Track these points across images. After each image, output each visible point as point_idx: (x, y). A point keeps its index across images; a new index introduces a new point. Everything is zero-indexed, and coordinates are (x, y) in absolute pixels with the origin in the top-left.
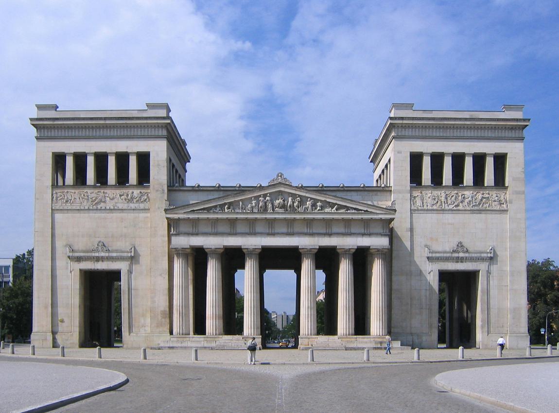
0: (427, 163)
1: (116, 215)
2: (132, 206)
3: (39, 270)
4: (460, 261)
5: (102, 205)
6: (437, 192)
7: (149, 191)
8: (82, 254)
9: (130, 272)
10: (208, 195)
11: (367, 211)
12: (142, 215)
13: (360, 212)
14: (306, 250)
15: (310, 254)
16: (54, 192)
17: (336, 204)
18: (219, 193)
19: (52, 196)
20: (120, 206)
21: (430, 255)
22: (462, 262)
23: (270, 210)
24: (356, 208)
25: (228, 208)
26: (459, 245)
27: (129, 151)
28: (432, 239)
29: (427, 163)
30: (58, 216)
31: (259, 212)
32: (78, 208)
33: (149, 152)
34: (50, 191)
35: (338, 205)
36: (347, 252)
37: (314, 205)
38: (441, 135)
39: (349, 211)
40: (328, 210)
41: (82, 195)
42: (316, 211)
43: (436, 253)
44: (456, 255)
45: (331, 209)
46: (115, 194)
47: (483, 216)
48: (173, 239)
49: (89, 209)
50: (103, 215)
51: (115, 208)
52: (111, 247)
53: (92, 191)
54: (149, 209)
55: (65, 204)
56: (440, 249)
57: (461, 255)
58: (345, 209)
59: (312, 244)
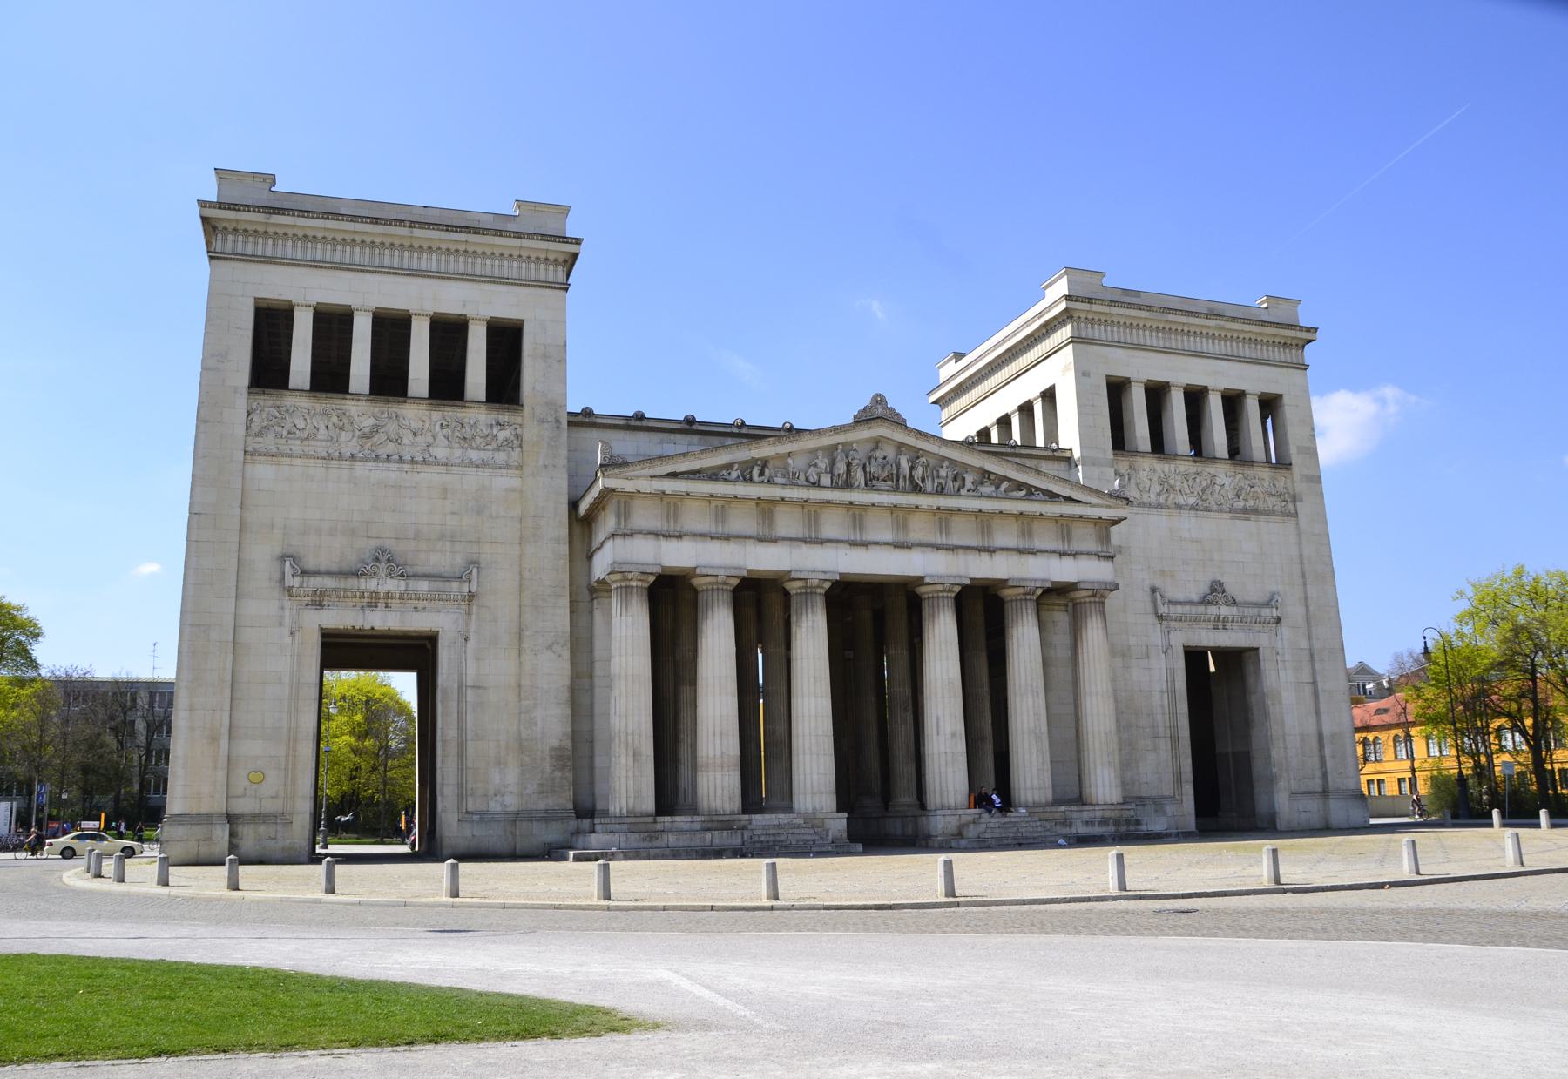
0: (1137, 402)
1: (431, 476)
2: (475, 455)
3: (199, 625)
4: (1220, 624)
6: (1162, 467)
7: (519, 420)
10: (661, 443)
11: (1069, 499)
12: (503, 482)
13: (1056, 499)
14: (940, 588)
15: (947, 597)
18: (688, 438)
19: (247, 416)
20: (440, 452)
21: (1163, 610)
24: (1047, 490)
25: (762, 474)
26: (1220, 590)
27: (468, 311)
28: (1162, 572)
29: (1137, 402)
30: (263, 471)
31: (835, 486)
32: (324, 454)
33: (523, 321)
34: (242, 401)
35: (1010, 480)
36: (1028, 597)
38: (1161, 345)
39: (1033, 497)
40: (987, 489)
41: (335, 419)
42: (963, 492)
44: (1213, 610)
45: (993, 488)
46: (427, 425)
47: (1251, 525)
50: (390, 473)
51: (427, 456)
52: (409, 566)
53: (359, 408)
54: (520, 467)
55: (283, 441)
56: (1180, 597)
57: (1224, 611)
58: (1023, 493)
59: (954, 571)
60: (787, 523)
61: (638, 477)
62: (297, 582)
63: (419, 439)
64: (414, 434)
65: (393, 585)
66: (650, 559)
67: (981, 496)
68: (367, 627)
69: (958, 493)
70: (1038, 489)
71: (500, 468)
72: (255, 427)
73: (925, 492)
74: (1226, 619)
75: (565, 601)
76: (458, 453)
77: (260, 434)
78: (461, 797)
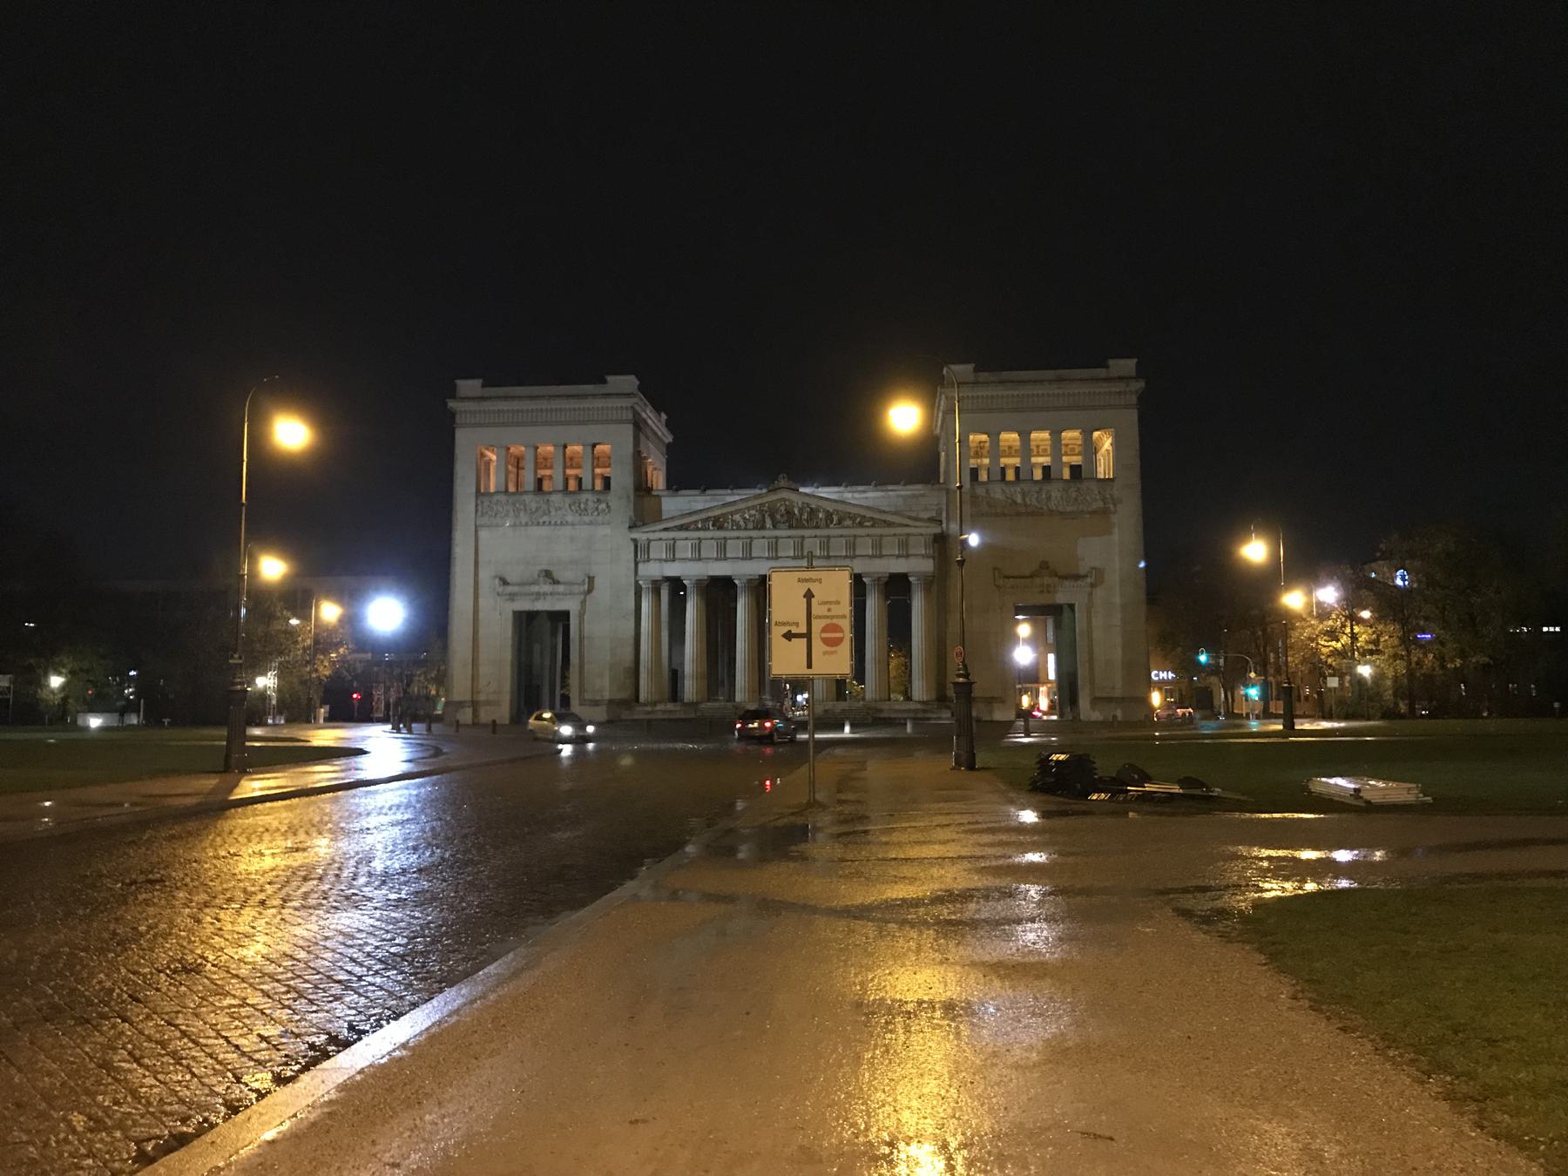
1: (567, 531)
2: (586, 519)
5: (545, 518)
8: (516, 589)
9: (581, 615)
16: (479, 502)
17: (859, 515)
20: (569, 518)
21: (1000, 582)
22: (1049, 592)
23: (769, 524)
31: (755, 528)
37: (829, 516)
42: (832, 526)
43: (1008, 577)
44: (1038, 581)
48: (641, 566)
49: (526, 524)
60: (734, 549)
61: (647, 532)
62: (500, 589)
63: (559, 512)
64: (556, 510)
65: (547, 588)
66: (657, 574)
67: (843, 527)
68: (535, 609)
69: (828, 526)
70: (880, 520)
71: (599, 524)
72: (479, 513)
73: (808, 528)
74: (1049, 586)
75: (633, 593)
76: (577, 518)
77: (482, 516)
78: (582, 690)
